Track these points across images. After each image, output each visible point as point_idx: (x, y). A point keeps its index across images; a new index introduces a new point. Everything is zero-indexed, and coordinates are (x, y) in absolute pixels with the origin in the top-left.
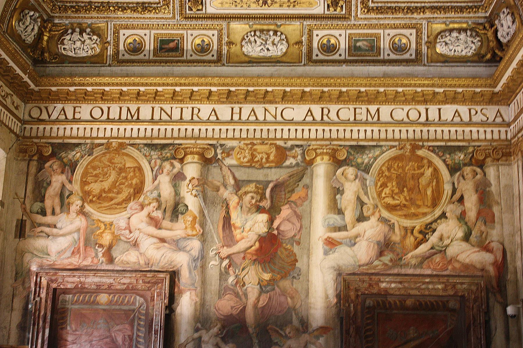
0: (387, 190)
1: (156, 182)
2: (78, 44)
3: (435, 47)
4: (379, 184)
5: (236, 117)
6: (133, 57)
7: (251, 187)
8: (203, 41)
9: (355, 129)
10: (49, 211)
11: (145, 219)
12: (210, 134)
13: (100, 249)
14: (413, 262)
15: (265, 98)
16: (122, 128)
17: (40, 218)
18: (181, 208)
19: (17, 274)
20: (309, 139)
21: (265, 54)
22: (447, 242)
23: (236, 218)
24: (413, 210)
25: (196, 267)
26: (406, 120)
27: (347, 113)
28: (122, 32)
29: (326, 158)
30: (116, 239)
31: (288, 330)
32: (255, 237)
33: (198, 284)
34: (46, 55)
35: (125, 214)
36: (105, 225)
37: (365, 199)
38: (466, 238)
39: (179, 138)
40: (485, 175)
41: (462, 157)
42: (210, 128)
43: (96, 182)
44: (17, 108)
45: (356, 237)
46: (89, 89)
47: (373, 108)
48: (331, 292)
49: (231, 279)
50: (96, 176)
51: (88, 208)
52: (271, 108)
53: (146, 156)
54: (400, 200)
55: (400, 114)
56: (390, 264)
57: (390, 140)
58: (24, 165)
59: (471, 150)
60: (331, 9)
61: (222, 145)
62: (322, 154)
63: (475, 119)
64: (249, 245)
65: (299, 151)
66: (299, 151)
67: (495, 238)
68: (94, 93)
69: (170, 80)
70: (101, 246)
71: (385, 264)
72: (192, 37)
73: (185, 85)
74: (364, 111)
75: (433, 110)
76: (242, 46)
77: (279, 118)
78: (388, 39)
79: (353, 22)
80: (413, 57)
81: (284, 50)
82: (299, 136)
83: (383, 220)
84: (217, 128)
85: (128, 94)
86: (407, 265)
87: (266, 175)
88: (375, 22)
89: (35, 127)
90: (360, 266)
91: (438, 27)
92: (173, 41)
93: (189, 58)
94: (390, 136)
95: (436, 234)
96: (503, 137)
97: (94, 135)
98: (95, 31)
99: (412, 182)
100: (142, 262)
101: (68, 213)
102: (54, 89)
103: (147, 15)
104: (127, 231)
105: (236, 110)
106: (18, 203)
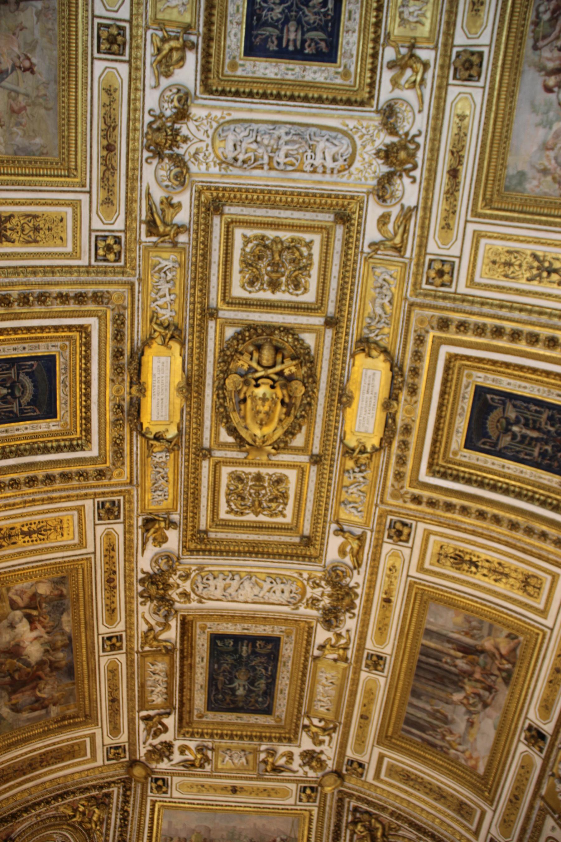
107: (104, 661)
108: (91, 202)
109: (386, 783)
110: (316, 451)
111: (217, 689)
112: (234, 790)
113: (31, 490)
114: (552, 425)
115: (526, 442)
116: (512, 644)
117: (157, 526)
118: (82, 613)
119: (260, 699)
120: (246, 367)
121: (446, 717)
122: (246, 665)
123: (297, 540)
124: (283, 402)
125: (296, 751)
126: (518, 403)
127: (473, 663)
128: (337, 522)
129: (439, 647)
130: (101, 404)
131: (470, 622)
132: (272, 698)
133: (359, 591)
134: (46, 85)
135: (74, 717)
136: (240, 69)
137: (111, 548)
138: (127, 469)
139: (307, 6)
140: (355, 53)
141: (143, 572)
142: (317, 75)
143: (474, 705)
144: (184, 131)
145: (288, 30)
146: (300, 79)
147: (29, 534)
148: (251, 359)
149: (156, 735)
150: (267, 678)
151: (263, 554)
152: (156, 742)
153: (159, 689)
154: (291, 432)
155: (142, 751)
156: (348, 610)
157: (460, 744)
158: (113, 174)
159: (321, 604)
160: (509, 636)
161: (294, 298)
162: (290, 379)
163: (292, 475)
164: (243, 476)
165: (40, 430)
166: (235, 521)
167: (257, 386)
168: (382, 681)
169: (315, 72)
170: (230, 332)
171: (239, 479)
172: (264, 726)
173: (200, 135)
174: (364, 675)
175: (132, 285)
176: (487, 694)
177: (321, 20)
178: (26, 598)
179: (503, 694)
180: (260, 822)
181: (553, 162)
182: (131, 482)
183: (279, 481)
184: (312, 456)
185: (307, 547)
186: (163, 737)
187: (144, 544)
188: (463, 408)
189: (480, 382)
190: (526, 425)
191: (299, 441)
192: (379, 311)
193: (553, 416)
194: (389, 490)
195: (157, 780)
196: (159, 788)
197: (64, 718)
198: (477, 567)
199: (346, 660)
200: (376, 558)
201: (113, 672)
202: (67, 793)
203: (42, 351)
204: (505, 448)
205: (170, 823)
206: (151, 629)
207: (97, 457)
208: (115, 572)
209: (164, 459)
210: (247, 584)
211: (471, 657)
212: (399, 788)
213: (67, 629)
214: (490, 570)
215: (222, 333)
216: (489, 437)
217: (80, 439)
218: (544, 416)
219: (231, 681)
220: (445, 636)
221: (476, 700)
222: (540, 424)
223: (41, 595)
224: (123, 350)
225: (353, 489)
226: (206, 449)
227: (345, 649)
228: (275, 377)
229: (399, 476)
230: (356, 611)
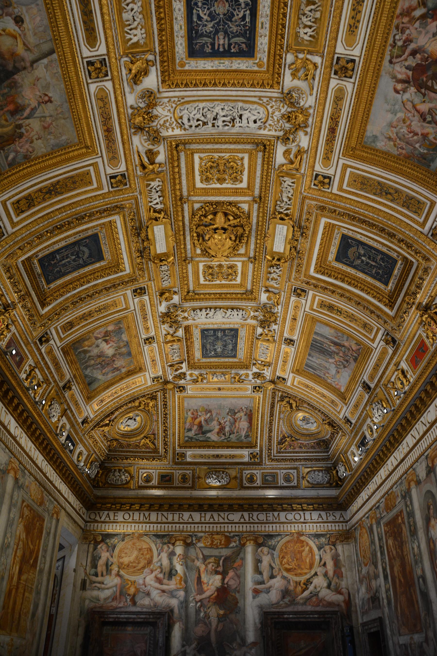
0: (285, 560)
6: (146, 485)
7: (212, 560)
10: (100, 574)
11: (154, 579)
17: (94, 578)
18: (174, 572)
19: (81, 612)
20: (242, 532)
22: (318, 589)
23: (204, 578)
24: (299, 571)
25: (182, 607)
26: (294, 520)
28: (140, 471)
29: (252, 542)
31: (234, 645)
32: (215, 589)
33: (184, 618)
35: (142, 576)
37: (273, 565)
38: (329, 587)
45: (270, 588)
48: (257, 621)
49: (202, 614)
58: (86, 546)
59: (328, 536)
60: (253, 460)
61: (195, 535)
62: (250, 540)
64: (211, 593)
65: (237, 538)
67: (344, 587)
70: (129, 595)
72: (178, 474)
78: (282, 475)
82: (237, 530)
83: (284, 578)
86: (298, 604)
87: (220, 553)
90: (273, 605)
95: (313, 585)
96: (344, 528)
99: (298, 555)
100: (152, 605)
101: (111, 574)
106: (82, 569)
108: (103, 161)
112: (219, 389)
116: (358, 347)
122: (221, 339)
125: (250, 373)
133: (279, 315)
134: (61, 106)
136: (187, 65)
139: (231, 21)
140: (266, 50)
142: (241, 65)
144: (155, 112)
145: (218, 38)
146: (229, 68)
158: (114, 144)
159: (259, 318)
160: (356, 343)
161: (234, 186)
169: (239, 64)
170: (197, 206)
171: (210, 267)
173: (166, 113)
174: (283, 346)
175: (136, 199)
177: (241, 30)
178: (103, 334)
180: (233, 401)
181: (395, 135)
186: (180, 371)
189: (345, 232)
190: (369, 258)
191: (242, 251)
192: (285, 199)
194: (293, 276)
195: (179, 387)
202: (135, 399)
203: (90, 233)
205: (188, 404)
218: (379, 257)
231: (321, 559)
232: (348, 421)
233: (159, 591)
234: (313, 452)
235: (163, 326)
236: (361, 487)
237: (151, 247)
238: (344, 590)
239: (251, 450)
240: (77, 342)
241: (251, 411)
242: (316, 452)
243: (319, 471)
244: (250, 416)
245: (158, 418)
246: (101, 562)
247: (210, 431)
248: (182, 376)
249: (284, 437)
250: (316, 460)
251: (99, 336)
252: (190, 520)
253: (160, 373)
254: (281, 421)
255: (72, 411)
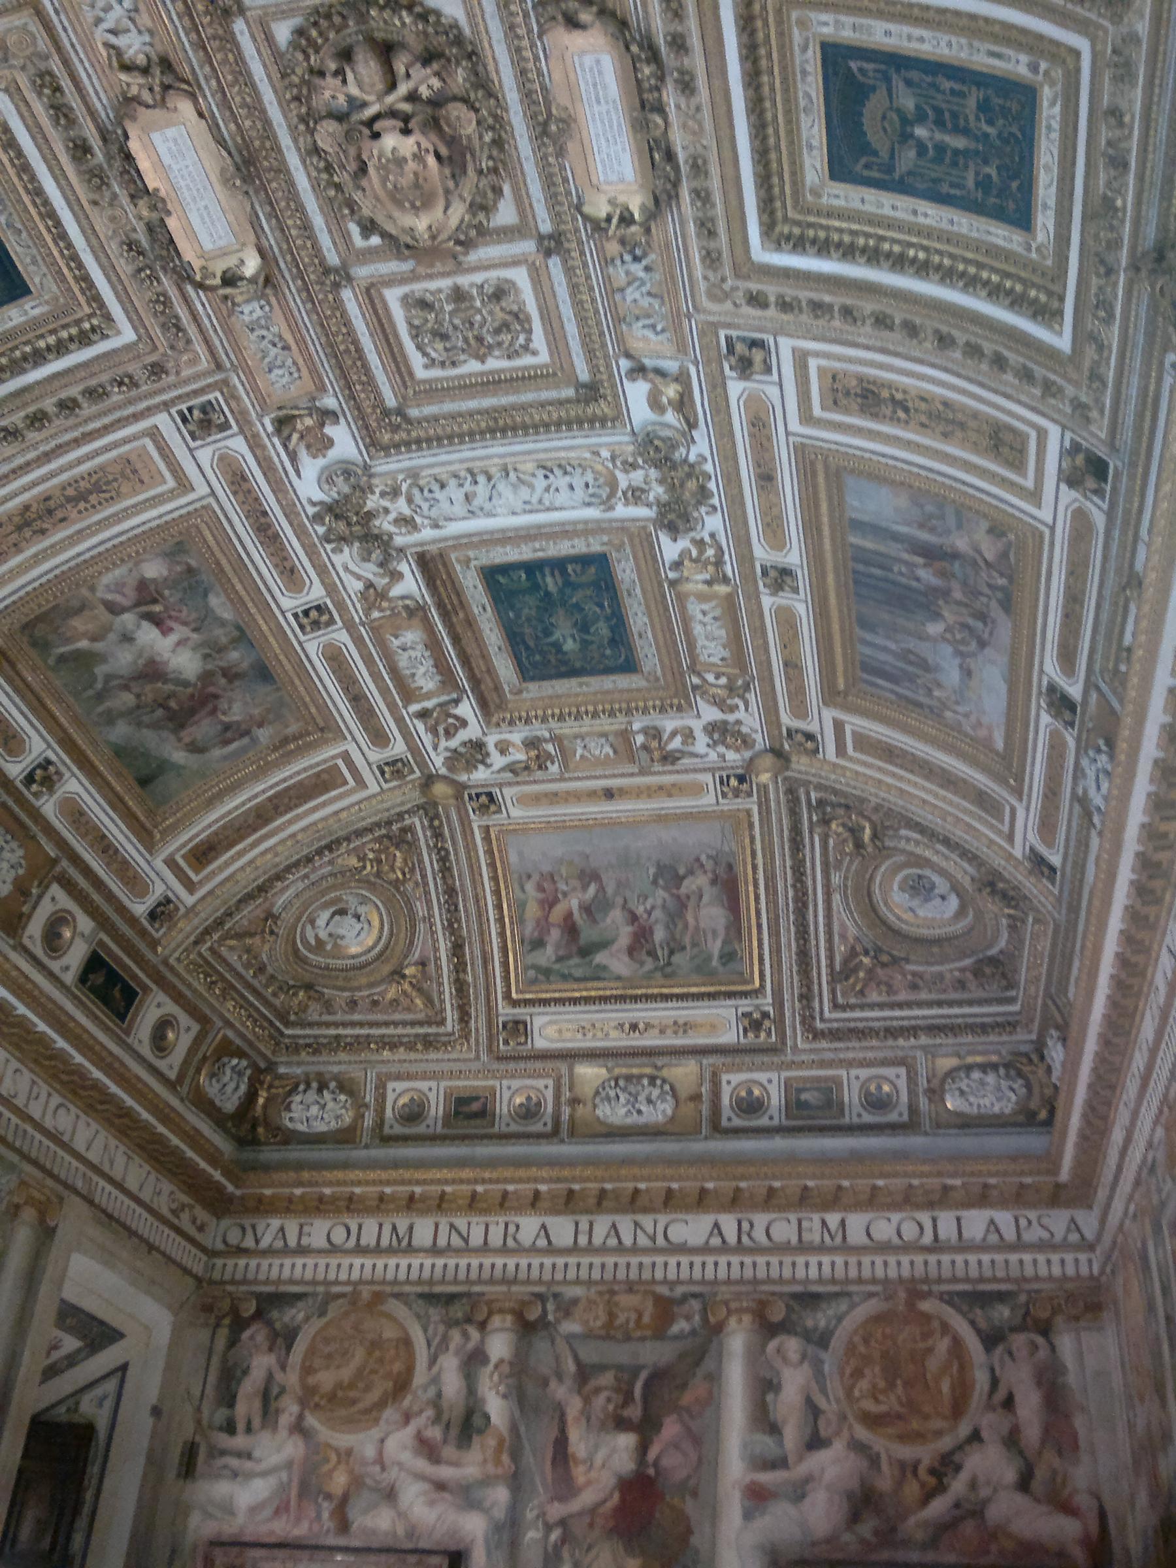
0: (864, 1384)
1: (435, 1369)
2: (314, 1110)
3: (943, 1101)
4: (848, 1371)
5: (583, 1240)
6: (407, 1131)
7: (607, 1379)
8: (529, 1098)
9: (801, 1260)
10: (241, 1426)
12: (535, 1273)
13: (326, 1504)
14: (919, 1535)
15: (634, 1203)
16: (380, 1263)
17: (223, 1440)
18: (477, 1421)
20: (715, 1282)
21: (634, 1119)
22: (984, 1492)
24: (915, 1424)
26: (896, 1240)
27: (784, 1229)
28: (390, 1085)
29: (747, 1319)
30: (357, 1482)
34: (261, 1130)
35: (375, 1433)
36: (339, 1455)
37: (822, 1403)
38: (1024, 1484)
39: (480, 1281)
40: (1053, 1349)
41: (1006, 1312)
42: (536, 1262)
43: (327, 1368)
44: (201, 1229)
46: (327, 1191)
47: (833, 1219)
50: (329, 1356)
51: (311, 1421)
52: (647, 1221)
53: (418, 1316)
54: (889, 1404)
55: (884, 1229)
56: (874, 1540)
57: (866, 1282)
58: (204, 1335)
59: (1023, 1298)
61: (556, 1296)
62: (740, 1311)
63: (1029, 1236)
64: (601, 1495)
65: (696, 1305)
66: (696, 1305)
68: (334, 1199)
69: (467, 1173)
70: (329, 1497)
71: (863, 1541)
72: (510, 1093)
73: (491, 1181)
74: (817, 1224)
75: (947, 1222)
76: (595, 1106)
77: (660, 1241)
78: (856, 1086)
79: (789, 1057)
80: (906, 1117)
81: (669, 1112)
83: (857, 1446)
84: (548, 1261)
85: (393, 1198)
86: (906, 1543)
88: (830, 1055)
89: (230, 1262)
90: (813, 1544)
91: (946, 1063)
92: (477, 1098)
93: (504, 1129)
94: (866, 1273)
97: (332, 1276)
98: (345, 1086)
100: (400, 1531)
101: (275, 1428)
102: (268, 1192)
103: (433, 1056)
104: (378, 1468)
105: (584, 1226)
107: (313, 646)
109: (858, 762)
110: (546, 227)
111: (527, 648)
112: (609, 794)
113: (45, 433)
114: (990, 122)
115: (947, 160)
116: (1000, 545)
117: (299, 426)
118: (239, 587)
119: (608, 652)
120: (342, 99)
121: (925, 661)
122: (564, 603)
123: (570, 392)
124: (438, 156)
125: (697, 726)
126: (914, 75)
127: (943, 574)
128: (628, 355)
129: (882, 548)
130: (99, 251)
131: (922, 506)
132: (630, 649)
133: (708, 467)
135: (301, 736)
137: (238, 480)
138: (199, 348)
141: (314, 504)
143: (963, 642)
147: (82, 497)
148: (344, 81)
149: (449, 734)
150: (608, 619)
151: (514, 429)
152: (454, 743)
153: (422, 670)
154: (482, 206)
155: (438, 762)
156: (700, 503)
157: (957, 703)
160: (991, 531)
162: (437, 102)
163: (520, 277)
164: (429, 298)
165: (10, 324)
166: (447, 379)
167: (376, 136)
168: (801, 609)
170: (283, 32)
171: (424, 305)
172: (629, 691)
176: (979, 625)
179: (1004, 629)
180: (668, 834)
182: (219, 366)
183: (499, 293)
184: (541, 238)
185: (592, 403)
186: (463, 735)
187: (293, 457)
188: (808, 95)
190: (940, 123)
191: (505, 214)
193: (987, 100)
195: (478, 795)
196: (483, 809)
197: (285, 741)
198: (906, 410)
199: (725, 580)
200: (720, 406)
201: (335, 658)
204: (909, 173)
205: (520, 854)
206: (369, 585)
207: (135, 344)
208: (265, 513)
209: (259, 313)
210: (501, 486)
211: (938, 565)
212: (880, 769)
213: (227, 615)
214: (930, 415)
215: (269, 39)
216: (875, 153)
217: (90, 316)
218: (972, 103)
219: (547, 633)
220: (886, 530)
221: (966, 634)
222: (966, 120)
223: (154, 580)
224: (85, 140)
225: (631, 294)
226: (336, 271)
227: (719, 563)
228: (406, 107)
229: (711, 259)
230: (715, 501)
231: (995, 1382)
232: (1039, 863)
233: (426, 1486)
234: (959, 1003)
235: (337, 559)
236: (1108, 1104)
237: (172, 223)
238: (1083, 1501)
239: (745, 1005)
240: (40, 619)
241: (730, 867)
242: (971, 1003)
243: (984, 1068)
244: (729, 887)
245: (430, 907)
246: (249, 1387)
247: (603, 945)
248: (476, 752)
249: (853, 953)
250: (971, 1028)
251: (118, 598)
252: (542, 1242)
253: (399, 747)
254: (837, 898)
255: (87, 871)
